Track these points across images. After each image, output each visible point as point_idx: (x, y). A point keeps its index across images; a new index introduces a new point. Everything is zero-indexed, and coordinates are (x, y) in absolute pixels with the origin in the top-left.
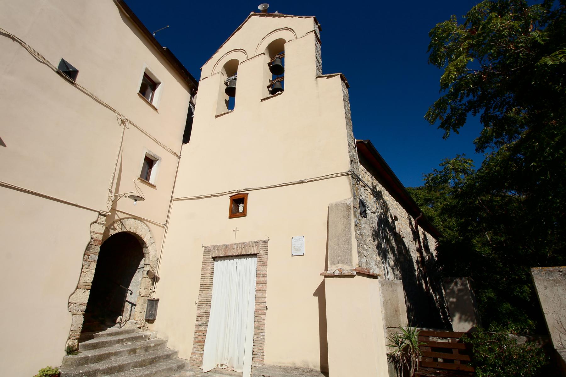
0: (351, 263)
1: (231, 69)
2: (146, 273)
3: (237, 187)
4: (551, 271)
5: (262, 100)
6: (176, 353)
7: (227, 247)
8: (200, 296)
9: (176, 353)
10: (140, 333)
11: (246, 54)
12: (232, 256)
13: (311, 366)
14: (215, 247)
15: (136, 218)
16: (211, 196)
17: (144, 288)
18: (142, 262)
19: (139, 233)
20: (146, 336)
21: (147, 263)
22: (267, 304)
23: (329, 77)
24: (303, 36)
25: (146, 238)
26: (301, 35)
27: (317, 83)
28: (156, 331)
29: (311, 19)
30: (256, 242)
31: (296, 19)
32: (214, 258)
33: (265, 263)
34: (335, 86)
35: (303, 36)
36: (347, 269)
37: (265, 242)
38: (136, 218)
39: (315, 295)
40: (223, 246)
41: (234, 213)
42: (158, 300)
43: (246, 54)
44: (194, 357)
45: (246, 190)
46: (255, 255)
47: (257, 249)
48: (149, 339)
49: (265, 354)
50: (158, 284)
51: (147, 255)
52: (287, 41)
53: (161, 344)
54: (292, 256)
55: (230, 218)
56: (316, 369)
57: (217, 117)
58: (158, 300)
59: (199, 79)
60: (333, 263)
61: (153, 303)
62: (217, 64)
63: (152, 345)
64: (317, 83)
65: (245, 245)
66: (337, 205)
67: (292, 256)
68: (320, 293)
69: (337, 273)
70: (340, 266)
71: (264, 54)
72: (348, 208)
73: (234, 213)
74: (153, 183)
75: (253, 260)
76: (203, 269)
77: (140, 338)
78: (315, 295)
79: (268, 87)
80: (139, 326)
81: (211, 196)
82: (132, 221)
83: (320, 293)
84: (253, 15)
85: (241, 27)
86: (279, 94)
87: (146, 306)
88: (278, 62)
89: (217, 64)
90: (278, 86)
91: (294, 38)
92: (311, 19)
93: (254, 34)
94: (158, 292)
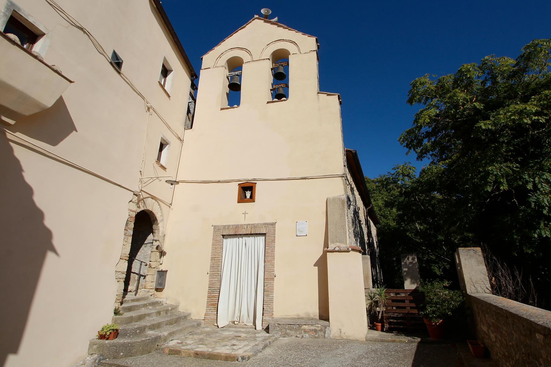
0: (346, 242)
1: (235, 65)
2: (155, 247)
3: (247, 176)
4: (469, 250)
5: (268, 102)
6: (190, 314)
7: (237, 227)
8: (212, 267)
9: (190, 314)
10: (153, 299)
11: (251, 55)
12: (241, 235)
13: (312, 316)
14: (225, 226)
15: (153, 198)
16: (219, 182)
17: (154, 260)
18: (150, 237)
19: (154, 211)
20: (160, 302)
21: (156, 238)
22: (276, 273)
23: (328, 95)
24: (306, 53)
25: (158, 216)
26: (303, 52)
27: (318, 98)
28: (167, 297)
29: (313, 39)
30: (265, 224)
31: (300, 35)
32: (223, 236)
33: (274, 241)
34: (332, 102)
35: (306, 53)
36: (343, 246)
37: (273, 224)
38: (153, 198)
39: (315, 265)
40: (233, 225)
41: (242, 199)
42: (167, 271)
43: (251, 55)
44: (208, 317)
45: (255, 180)
46: (264, 234)
47: (266, 229)
48: (162, 304)
49: (274, 310)
50: (164, 258)
51: (156, 231)
52: (291, 53)
53: (174, 308)
54: (297, 236)
55: (238, 202)
56: (316, 317)
57: (222, 109)
58: (167, 271)
59: (200, 68)
60: (333, 242)
61: (162, 274)
62: (220, 57)
63: (170, 309)
64: (318, 98)
65: (254, 226)
66: (334, 199)
67: (297, 236)
68: (322, 265)
69: (337, 249)
70: (338, 244)
71: (269, 59)
72: (343, 202)
73: (242, 199)
74: (164, 165)
75: (262, 238)
76: (213, 245)
77: (154, 304)
78: (315, 265)
79: (271, 90)
80: (151, 294)
81: (219, 182)
82: (150, 199)
83: (322, 265)
84: (257, 18)
85: (245, 27)
86: (284, 100)
87: (155, 276)
88: (281, 70)
89: (220, 57)
90: (281, 91)
91: (298, 52)
92: (313, 39)
93: (257, 39)
94: (166, 264)
